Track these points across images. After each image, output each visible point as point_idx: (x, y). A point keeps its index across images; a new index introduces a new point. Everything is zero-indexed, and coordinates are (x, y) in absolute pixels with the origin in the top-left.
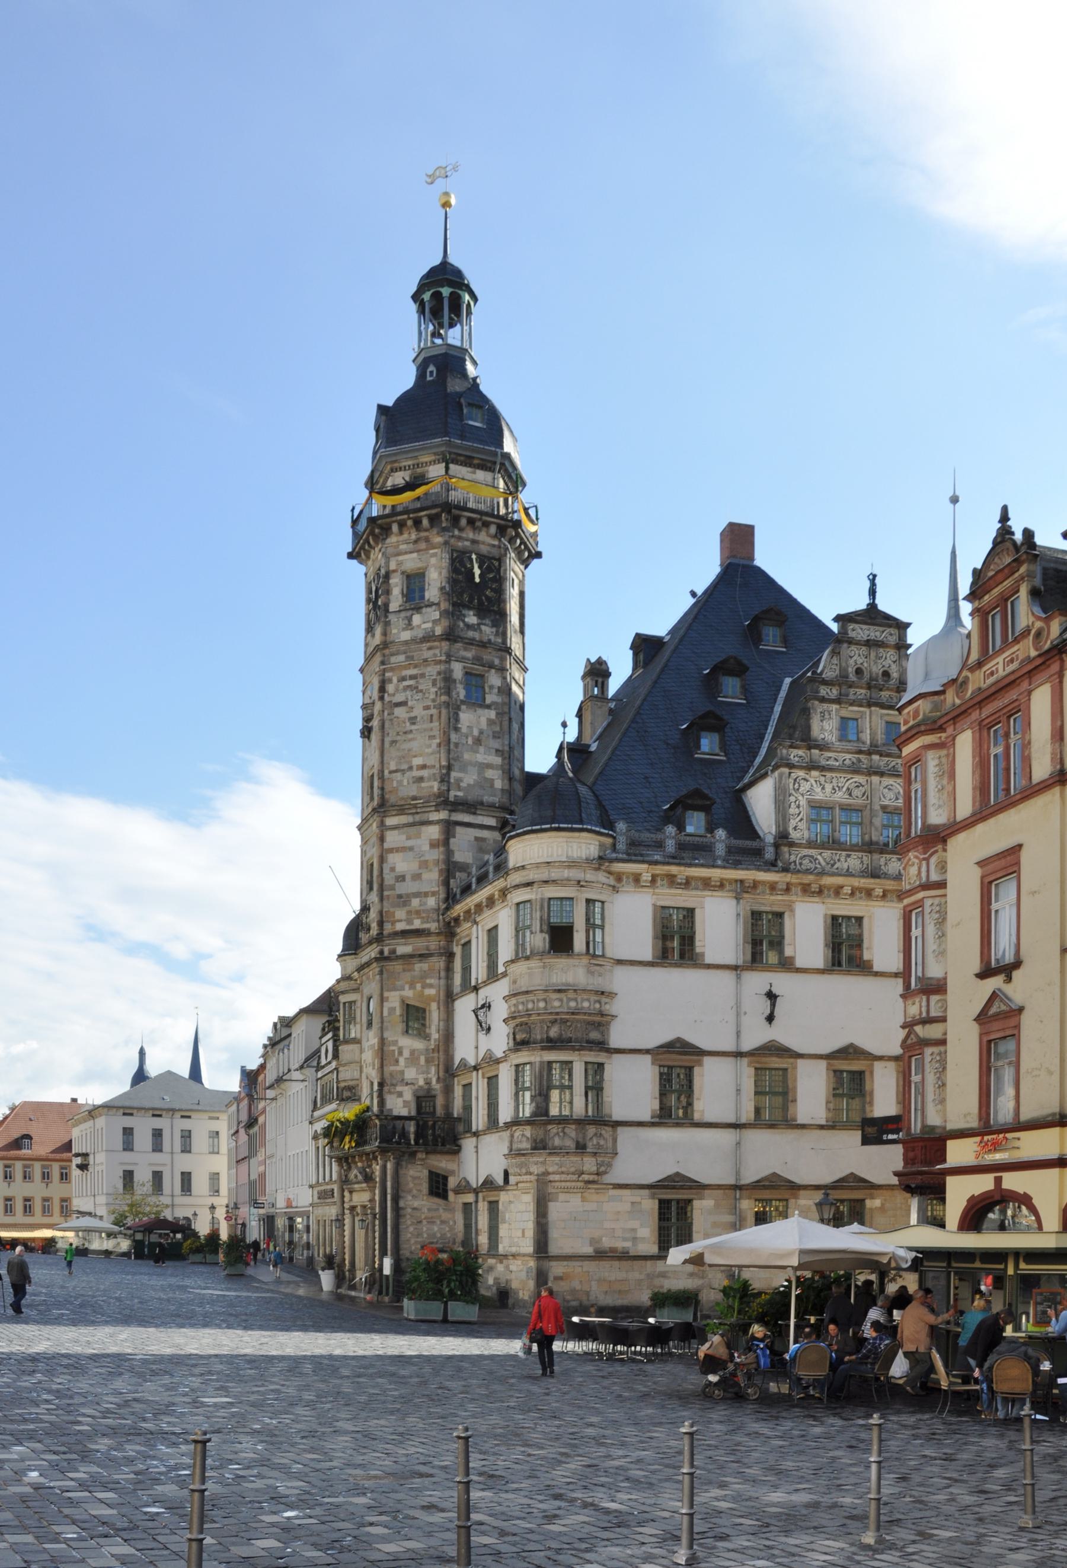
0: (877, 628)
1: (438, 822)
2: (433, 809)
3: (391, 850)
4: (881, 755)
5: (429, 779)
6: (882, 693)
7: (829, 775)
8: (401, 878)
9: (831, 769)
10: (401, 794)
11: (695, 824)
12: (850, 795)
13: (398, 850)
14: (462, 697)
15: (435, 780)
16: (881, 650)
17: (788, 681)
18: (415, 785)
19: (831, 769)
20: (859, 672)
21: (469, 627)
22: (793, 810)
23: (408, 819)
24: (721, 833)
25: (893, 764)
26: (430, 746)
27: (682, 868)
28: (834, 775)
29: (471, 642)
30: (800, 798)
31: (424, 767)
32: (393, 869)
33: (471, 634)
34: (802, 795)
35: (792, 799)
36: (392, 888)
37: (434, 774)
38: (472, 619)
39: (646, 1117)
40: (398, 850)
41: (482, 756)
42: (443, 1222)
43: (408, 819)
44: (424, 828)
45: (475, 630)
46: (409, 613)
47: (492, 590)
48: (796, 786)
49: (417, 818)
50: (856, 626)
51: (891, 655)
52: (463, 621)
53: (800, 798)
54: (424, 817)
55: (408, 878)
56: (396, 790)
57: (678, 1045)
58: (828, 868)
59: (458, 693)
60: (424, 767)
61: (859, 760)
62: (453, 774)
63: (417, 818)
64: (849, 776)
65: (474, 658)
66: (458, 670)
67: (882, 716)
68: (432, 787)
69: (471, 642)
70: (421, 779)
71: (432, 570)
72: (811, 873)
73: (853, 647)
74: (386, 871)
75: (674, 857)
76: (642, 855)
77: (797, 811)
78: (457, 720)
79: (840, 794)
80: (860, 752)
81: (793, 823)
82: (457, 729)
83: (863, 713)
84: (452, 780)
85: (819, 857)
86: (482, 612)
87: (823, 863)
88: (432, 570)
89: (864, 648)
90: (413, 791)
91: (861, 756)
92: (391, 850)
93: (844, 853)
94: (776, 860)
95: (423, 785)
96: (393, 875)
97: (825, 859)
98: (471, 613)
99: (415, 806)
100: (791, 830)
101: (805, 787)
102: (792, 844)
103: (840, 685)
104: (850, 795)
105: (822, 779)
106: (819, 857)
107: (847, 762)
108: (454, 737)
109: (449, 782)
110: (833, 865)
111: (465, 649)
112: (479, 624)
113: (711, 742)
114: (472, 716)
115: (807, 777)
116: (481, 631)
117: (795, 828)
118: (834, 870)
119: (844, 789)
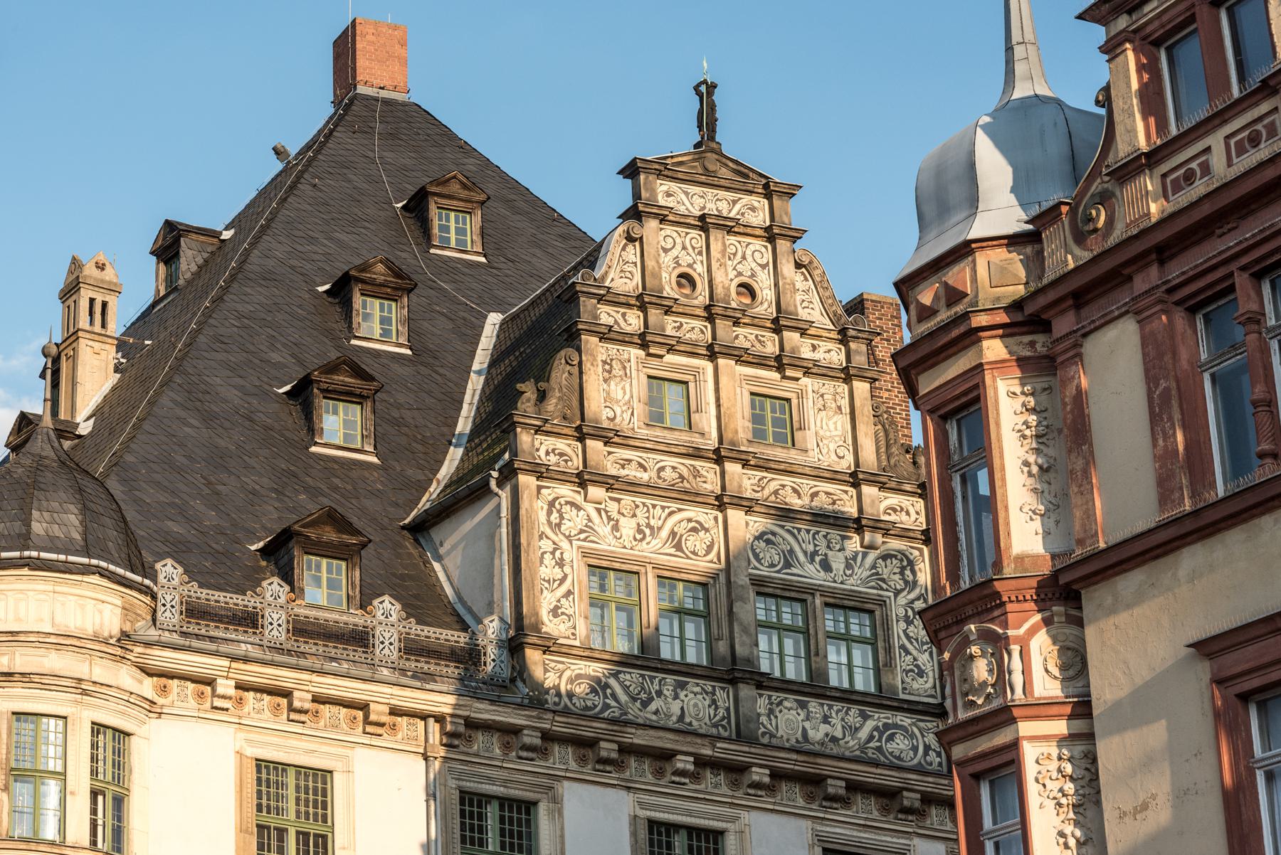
0: (722, 194)
6: (739, 330)
7: (627, 499)
9: (632, 487)
11: (323, 588)
12: (678, 547)
16: (732, 239)
17: (494, 319)
20: (686, 279)
22: (548, 570)
24: (387, 608)
25: (773, 486)
27: (305, 676)
28: (638, 500)
30: (565, 544)
34: (568, 537)
35: (546, 545)
48: (555, 517)
50: (673, 186)
51: (758, 250)
53: (565, 544)
58: (634, 711)
67: (748, 379)
72: (596, 718)
73: (669, 230)
75: (280, 650)
76: (212, 639)
77: (558, 573)
79: (656, 543)
83: (696, 372)
85: (612, 681)
87: (623, 698)
89: (694, 233)
94: (513, 680)
100: (545, 615)
101: (573, 522)
102: (549, 646)
103: (643, 307)
104: (678, 547)
106: (612, 681)
107: (668, 474)
110: (645, 704)
113: (346, 423)
115: (579, 499)
118: (648, 715)
119: (664, 533)
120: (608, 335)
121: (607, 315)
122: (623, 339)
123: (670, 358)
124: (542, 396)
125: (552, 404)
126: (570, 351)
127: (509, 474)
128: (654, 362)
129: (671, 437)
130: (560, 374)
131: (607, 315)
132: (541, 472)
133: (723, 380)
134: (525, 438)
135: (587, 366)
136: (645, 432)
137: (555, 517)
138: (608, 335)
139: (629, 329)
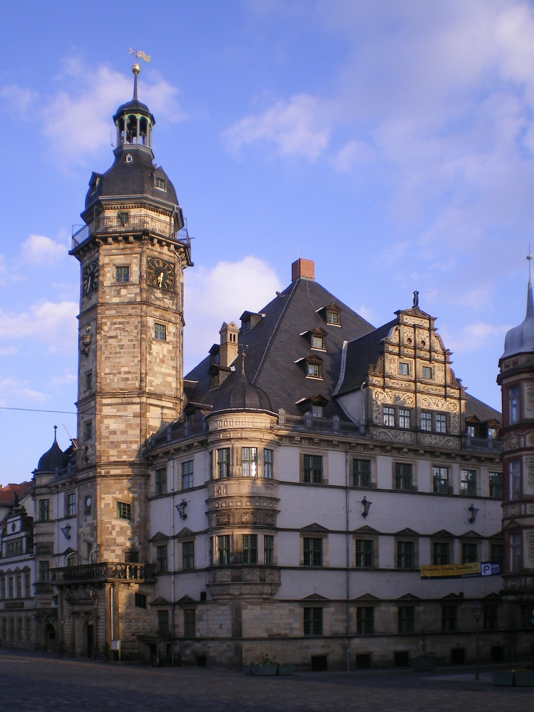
1: (140, 403)
2: (136, 396)
3: (107, 417)
4: (421, 383)
5: (133, 379)
8: (114, 433)
10: (113, 387)
13: (111, 417)
14: (153, 336)
15: (137, 380)
18: (123, 382)
19: (395, 389)
21: (157, 299)
23: (120, 400)
26: (133, 361)
29: (159, 307)
31: (129, 373)
32: (107, 427)
33: (158, 303)
36: (107, 437)
37: (136, 377)
38: (159, 294)
39: (297, 564)
40: (111, 417)
41: (164, 370)
42: (145, 621)
43: (120, 400)
44: (129, 406)
45: (160, 301)
46: (119, 288)
47: (170, 280)
49: (125, 400)
52: (154, 295)
54: (129, 400)
55: (118, 433)
56: (109, 384)
57: (315, 527)
59: (151, 334)
60: (129, 373)
61: (410, 385)
62: (148, 378)
63: (125, 400)
64: (404, 393)
65: (160, 316)
66: (151, 322)
68: (135, 384)
69: (159, 307)
70: (127, 379)
71: (134, 265)
74: (103, 428)
78: (151, 349)
80: (410, 381)
81: (375, 415)
82: (150, 354)
84: (147, 381)
86: (165, 291)
88: (134, 265)
90: (122, 385)
91: (410, 383)
92: (107, 417)
93: (402, 432)
95: (128, 382)
96: (108, 431)
97: (392, 434)
98: (159, 291)
99: (123, 394)
105: (390, 393)
108: (148, 358)
109: (146, 382)
111: (155, 311)
112: (163, 298)
114: (159, 347)
116: (164, 301)
117: (376, 418)
120: (391, 353)
121: (391, 348)
122: (394, 354)
123: (405, 358)
124: (375, 368)
125: (377, 369)
126: (382, 357)
127: (366, 386)
128: (401, 359)
129: (404, 377)
130: (379, 363)
131: (391, 348)
132: (374, 386)
133: (417, 364)
134: (370, 378)
135: (386, 360)
136: (398, 376)
137: (377, 396)
138: (391, 353)
139: (395, 352)
